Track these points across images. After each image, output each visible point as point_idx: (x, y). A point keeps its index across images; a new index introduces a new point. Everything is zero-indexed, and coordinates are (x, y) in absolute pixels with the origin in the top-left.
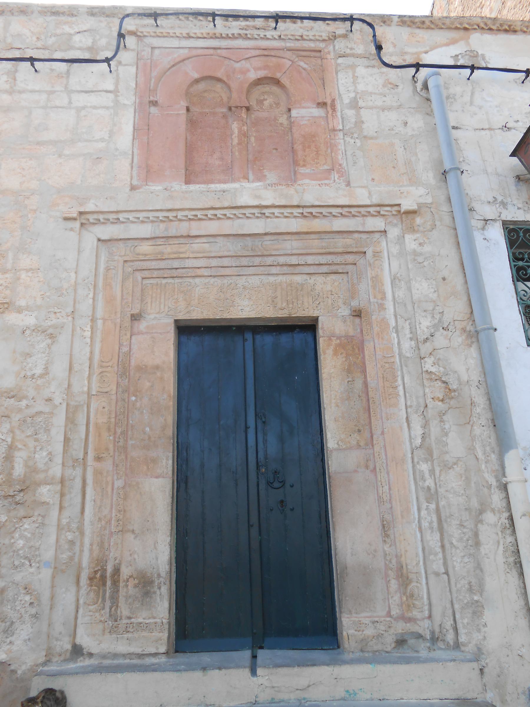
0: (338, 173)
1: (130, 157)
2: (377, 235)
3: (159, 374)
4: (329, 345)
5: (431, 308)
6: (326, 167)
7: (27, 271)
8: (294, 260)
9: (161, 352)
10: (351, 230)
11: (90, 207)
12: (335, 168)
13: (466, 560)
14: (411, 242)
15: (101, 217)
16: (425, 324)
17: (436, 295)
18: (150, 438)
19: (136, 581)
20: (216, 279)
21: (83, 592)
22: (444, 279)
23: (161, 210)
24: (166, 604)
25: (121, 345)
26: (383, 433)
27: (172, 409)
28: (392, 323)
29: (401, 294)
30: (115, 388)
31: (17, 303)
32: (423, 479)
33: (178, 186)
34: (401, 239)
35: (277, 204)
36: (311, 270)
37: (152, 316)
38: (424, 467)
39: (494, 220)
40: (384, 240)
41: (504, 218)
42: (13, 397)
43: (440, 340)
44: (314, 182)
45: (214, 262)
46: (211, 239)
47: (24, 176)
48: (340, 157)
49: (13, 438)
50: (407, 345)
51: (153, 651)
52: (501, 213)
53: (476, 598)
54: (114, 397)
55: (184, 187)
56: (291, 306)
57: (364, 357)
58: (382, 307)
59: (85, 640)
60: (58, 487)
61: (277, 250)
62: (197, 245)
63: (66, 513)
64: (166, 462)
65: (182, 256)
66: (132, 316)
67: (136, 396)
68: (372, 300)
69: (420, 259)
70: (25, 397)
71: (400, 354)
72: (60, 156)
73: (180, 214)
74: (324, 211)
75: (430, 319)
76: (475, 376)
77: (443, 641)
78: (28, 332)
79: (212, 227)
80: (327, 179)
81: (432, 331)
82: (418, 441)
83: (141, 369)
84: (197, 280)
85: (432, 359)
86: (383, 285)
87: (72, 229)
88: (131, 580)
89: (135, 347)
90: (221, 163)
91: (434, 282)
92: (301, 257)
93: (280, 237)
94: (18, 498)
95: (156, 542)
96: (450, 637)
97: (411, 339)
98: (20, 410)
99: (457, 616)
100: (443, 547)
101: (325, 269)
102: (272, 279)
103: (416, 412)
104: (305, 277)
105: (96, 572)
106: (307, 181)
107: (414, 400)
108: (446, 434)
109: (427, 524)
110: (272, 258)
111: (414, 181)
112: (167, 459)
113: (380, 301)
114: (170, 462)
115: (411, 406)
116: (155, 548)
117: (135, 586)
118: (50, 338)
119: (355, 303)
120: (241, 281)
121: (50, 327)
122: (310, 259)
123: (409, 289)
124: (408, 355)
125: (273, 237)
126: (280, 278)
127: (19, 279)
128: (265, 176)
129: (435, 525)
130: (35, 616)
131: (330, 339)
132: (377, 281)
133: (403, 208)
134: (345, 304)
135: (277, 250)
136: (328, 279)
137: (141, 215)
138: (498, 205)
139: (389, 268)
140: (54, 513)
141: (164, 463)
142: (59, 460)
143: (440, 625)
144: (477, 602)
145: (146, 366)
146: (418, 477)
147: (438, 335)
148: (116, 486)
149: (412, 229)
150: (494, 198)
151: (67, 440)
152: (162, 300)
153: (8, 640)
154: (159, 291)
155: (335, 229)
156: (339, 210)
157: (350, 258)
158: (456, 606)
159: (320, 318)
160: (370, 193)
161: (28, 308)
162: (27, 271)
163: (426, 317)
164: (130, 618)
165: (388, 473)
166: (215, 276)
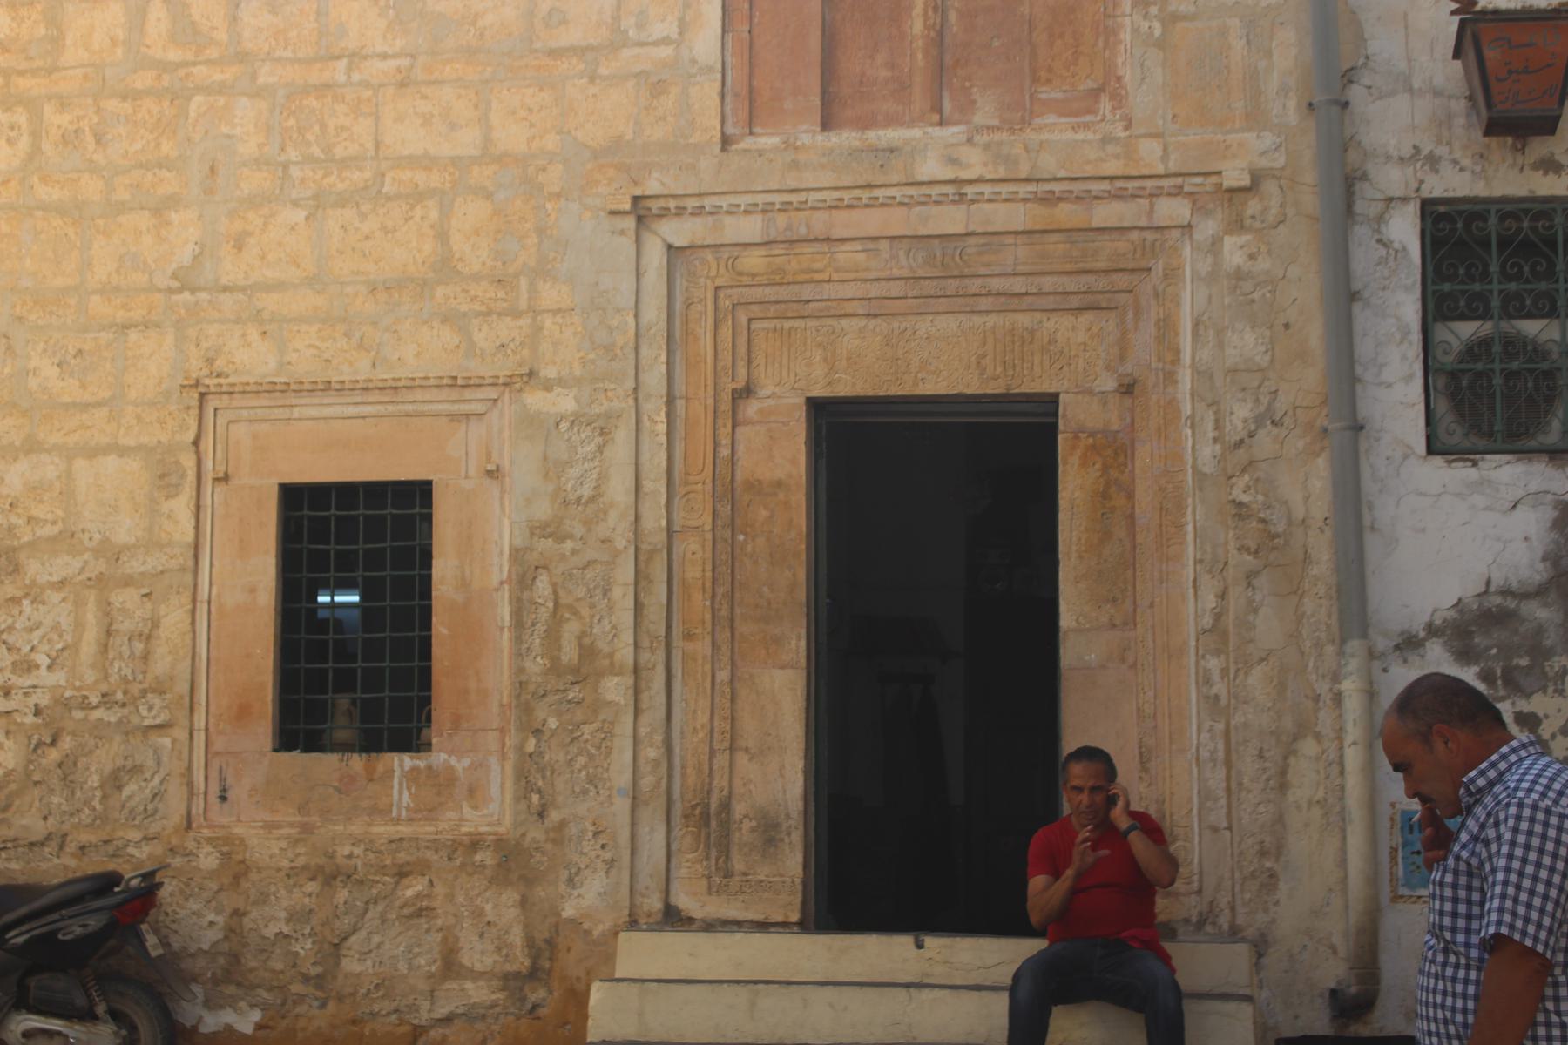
0: (1112, 98)
1: (719, 76)
2: (1176, 234)
3: (781, 496)
4: (1074, 448)
5: (1256, 384)
6: (1090, 84)
7: (556, 312)
8: (1018, 285)
9: (781, 457)
10: (1126, 224)
11: (652, 186)
12: (1109, 87)
13: (1262, 809)
14: (1234, 251)
15: (672, 204)
16: (1240, 413)
17: (1267, 358)
18: (769, 603)
19: (754, 823)
20: (879, 320)
21: (678, 832)
22: (1287, 326)
23: (778, 191)
24: (799, 858)
25: (716, 445)
26: (1152, 605)
27: (804, 557)
28: (1187, 409)
29: (1205, 354)
30: (710, 520)
31: (542, 374)
32: (1208, 681)
33: (810, 137)
34: (1216, 242)
35: (989, 176)
36: (1049, 302)
37: (767, 392)
38: (1213, 664)
39: (1405, 200)
40: (1188, 243)
41: (1425, 194)
42: (550, 535)
43: (1265, 442)
44: (1063, 120)
45: (875, 290)
46: (871, 245)
47: (532, 125)
48: (1120, 61)
49: (556, 603)
50: (1208, 452)
51: (780, 919)
52: (1422, 182)
53: (1268, 865)
54: (709, 536)
55: (819, 138)
56: (1010, 372)
57: (1133, 471)
58: (1170, 378)
59: (684, 901)
60: (630, 681)
61: (988, 265)
62: (847, 255)
63: (644, 719)
64: (796, 644)
65: (818, 277)
66: (734, 391)
67: (746, 534)
68: (1154, 365)
69: (1247, 286)
70: (571, 537)
71: (1194, 467)
72: (592, 80)
73: (813, 197)
74: (1077, 187)
75: (1250, 405)
76: (1320, 508)
77: (1214, 924)
78: (564, 426)
79: (872, 222)
80: (1089, 111)
81: (1253, 427)
82: (1207, 621)
83: (750, 486)
84: (845, 322)
85: (1247, 477)
86: (1177, 334)
87: (622, 233)
88: (746, 821)
89: (741, 449)
90: (890, 74)
91: (1268, 333)
92: (1030, 279)
93: (995, 239)
94: (571, 696)
95: (782, 768)
96: (1224, 922)
97: (1215, 440)
98: (563, 557)
99: (1237, 889)
100: (1228, 789)
101: (1075, 302)
102: (978, 320)
103: (1210, 572)
104: (1038, 315)
105: (693, 807)
106: (1051, 119)
107: (1209, 549)
108: (1255, 611)
109: (1207, 755)
110: (979, 281)
111: (1255, 118)
112: (799, 639)
113: (1168, 367)
114: (803, 643)
115: (1201, 561)
116: (782, 776)
117: (753, 830)
118: (601, 434)
119: (1128, 368)
120: (924, 326)
121: (599, 416)
122: (1048, 283)
123: (1221, 345)
124: (1206, 470)
125: (981, 240)
126: (992, 320)
127: (541, 328)
128: (974, 102)
129: (1221, 755)
130: (611, 863)
131: (1076, 437)
132: (1167, 326)
133: (1227, 184)
134: (1108, 368)
135: (988, 265)
136: (1081, 319)
137: (743, 200)
138: (1418, 165)
139: (1189, 302)
140: (628, 719)
141: (793, 646)
142: (628, 637)
143: (1211, 902)
144: (1269, 869)
145: (760, 482)
146: (1205, 679)
147: (1262, 433)
148: (718, 680)
149: (1237, 225)
150: (1415, 147)
151: (638, 607)
152: (785, 361)
153: (576, 893)
154: (778, 343)
155: (1096, 223)
156: (1105, 185)
157: (1122, 280)
158: (1237, 875)
159: (1062, 397)
160: (1165, 150)
161: (561, 382)
162: (556, 312)
163: (1244, 400)
164: (745, 874)
165: (1155, 671)
166: (876, 316)
